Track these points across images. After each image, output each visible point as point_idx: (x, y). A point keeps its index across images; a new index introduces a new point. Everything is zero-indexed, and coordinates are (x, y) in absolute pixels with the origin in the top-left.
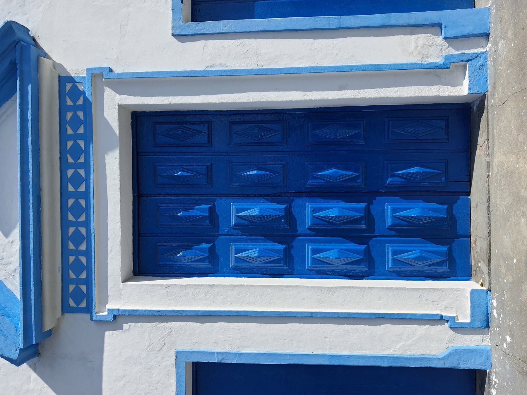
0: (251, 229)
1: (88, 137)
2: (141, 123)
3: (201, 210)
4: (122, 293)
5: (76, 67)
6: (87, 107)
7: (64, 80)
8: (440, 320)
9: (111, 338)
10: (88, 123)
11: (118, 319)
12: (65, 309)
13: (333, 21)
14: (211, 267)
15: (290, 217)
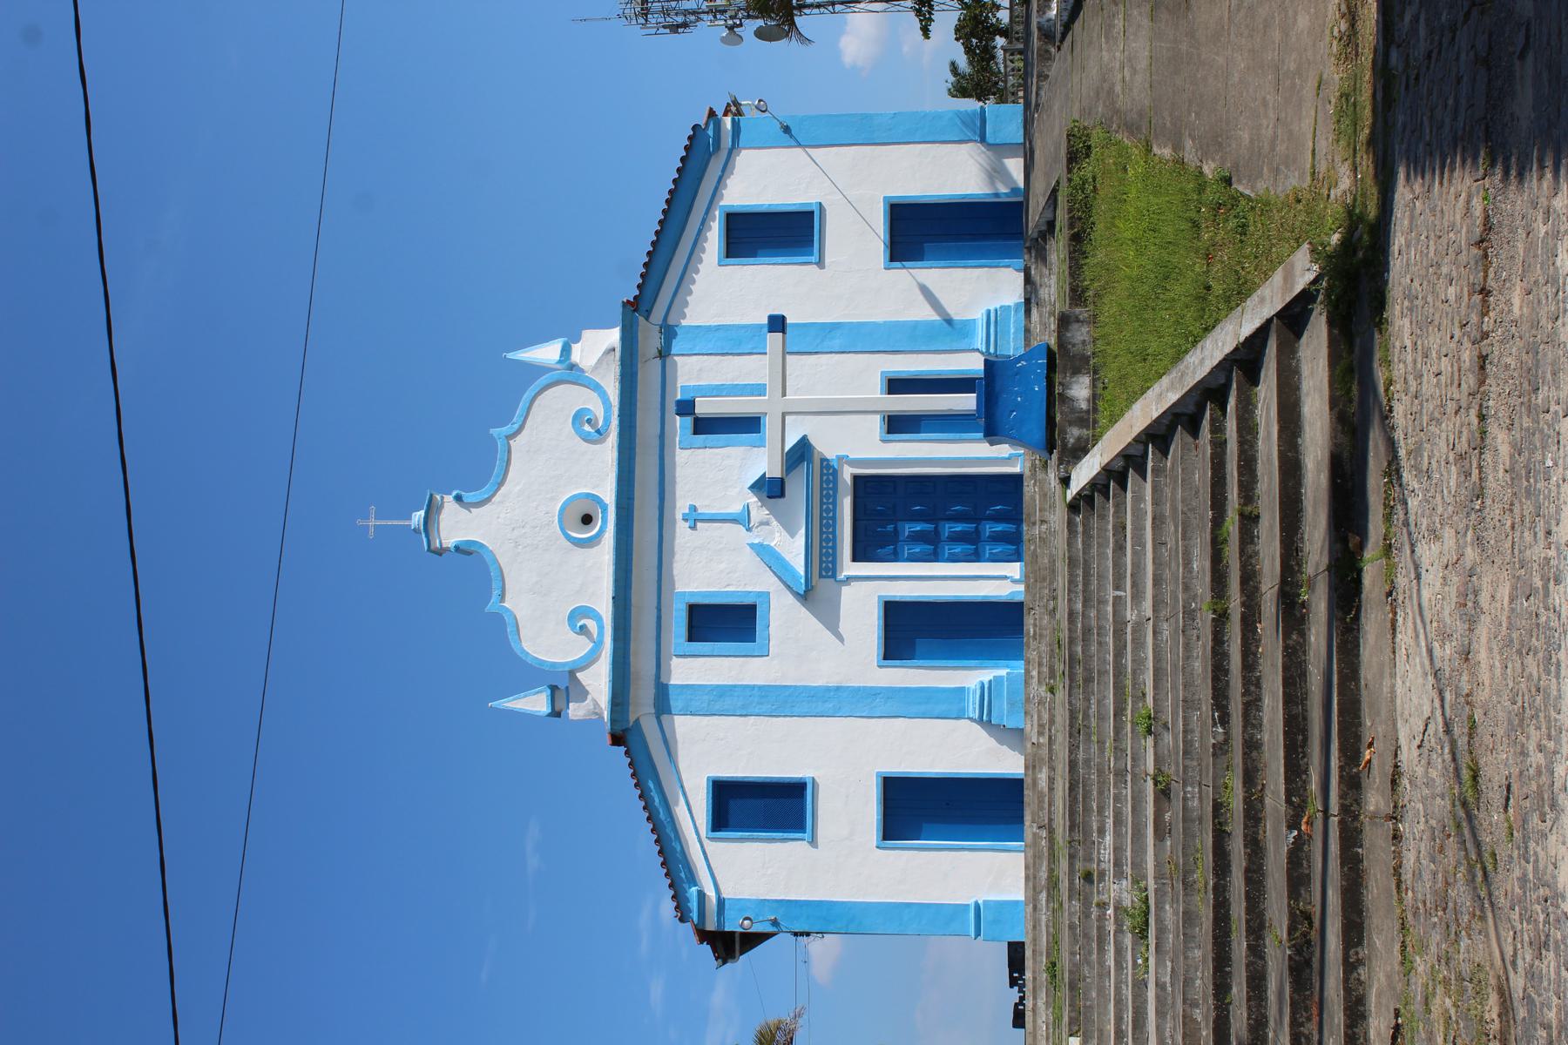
0: (917, 538)
1: (835, 489)
2: (856, 478)
3: (890, 528)
4: (849, 568)
5: (831, 455)
6: (835, 471)
7: (824, 460)
8: (1005, 578)
9: (845, 589)
10: (835, 482)
11: (849, 579)
12: (821, 576)
13: (958, 436)
14: (895, 557)
15: (936, 531)
